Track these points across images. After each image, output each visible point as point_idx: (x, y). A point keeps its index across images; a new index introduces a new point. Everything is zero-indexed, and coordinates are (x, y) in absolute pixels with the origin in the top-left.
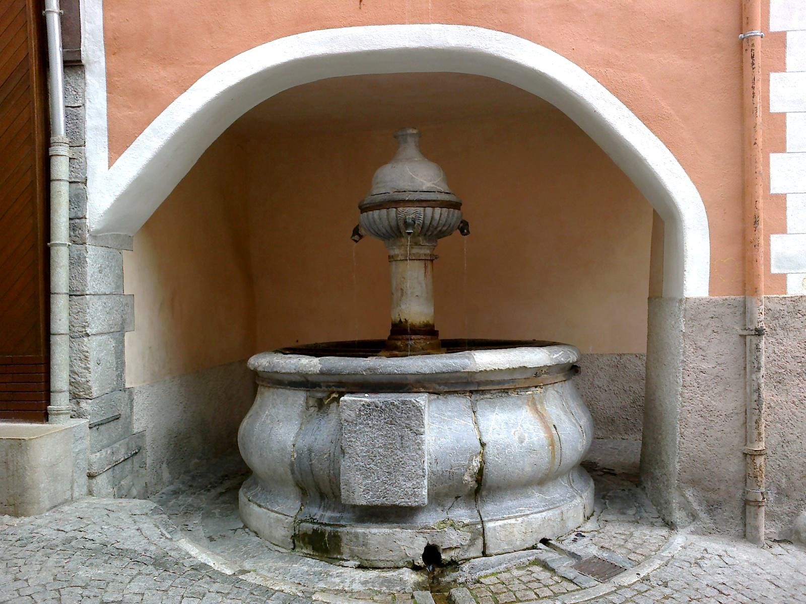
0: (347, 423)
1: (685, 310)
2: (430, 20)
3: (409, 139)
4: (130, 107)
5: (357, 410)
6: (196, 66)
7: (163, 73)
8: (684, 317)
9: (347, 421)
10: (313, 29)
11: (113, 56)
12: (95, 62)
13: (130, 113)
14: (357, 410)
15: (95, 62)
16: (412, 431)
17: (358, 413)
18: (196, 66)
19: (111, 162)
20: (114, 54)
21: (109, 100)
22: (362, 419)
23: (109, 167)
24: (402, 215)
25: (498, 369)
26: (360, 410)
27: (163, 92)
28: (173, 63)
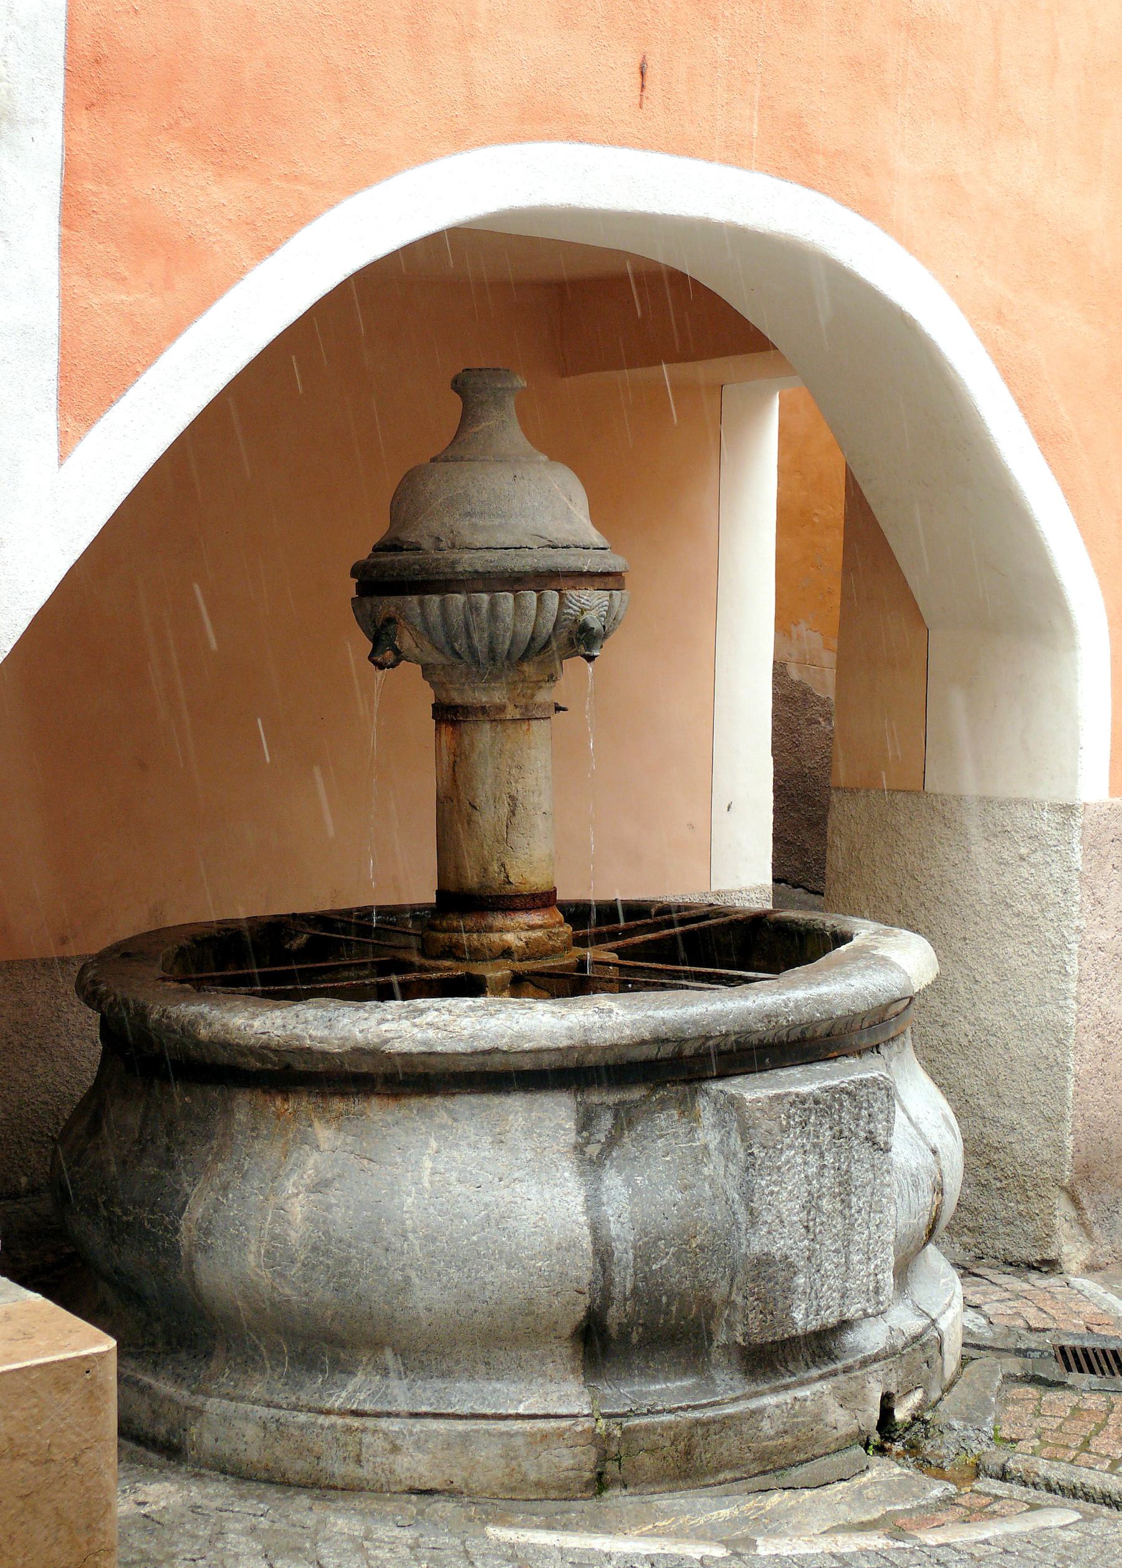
0: (765, 1150)
1: (1083, 827)
2: (753, 162)
3: (511, 402)
4: (124, 279)
5: (783, 1116)
6: (300, 187)
7: (218, 194)
8: (1082, 841)
9: (765, 1148)
10: (550, 137)
11: (84, 112)
12: (33, 121)
13: (124, 297)
14: (783, 1116)
15: (33, 121)
16: (876, 1147)
17: (784, 1123)
18: (300, 187)
19: (66, 444)
20: (90, 106)
21: (66, 250)
22: (792, 1136)
23: (62, 457)
24: (573, 610)
25: (195, 941)
26: (789, 1117)
27: (217, 248)
28: (244, 168)
